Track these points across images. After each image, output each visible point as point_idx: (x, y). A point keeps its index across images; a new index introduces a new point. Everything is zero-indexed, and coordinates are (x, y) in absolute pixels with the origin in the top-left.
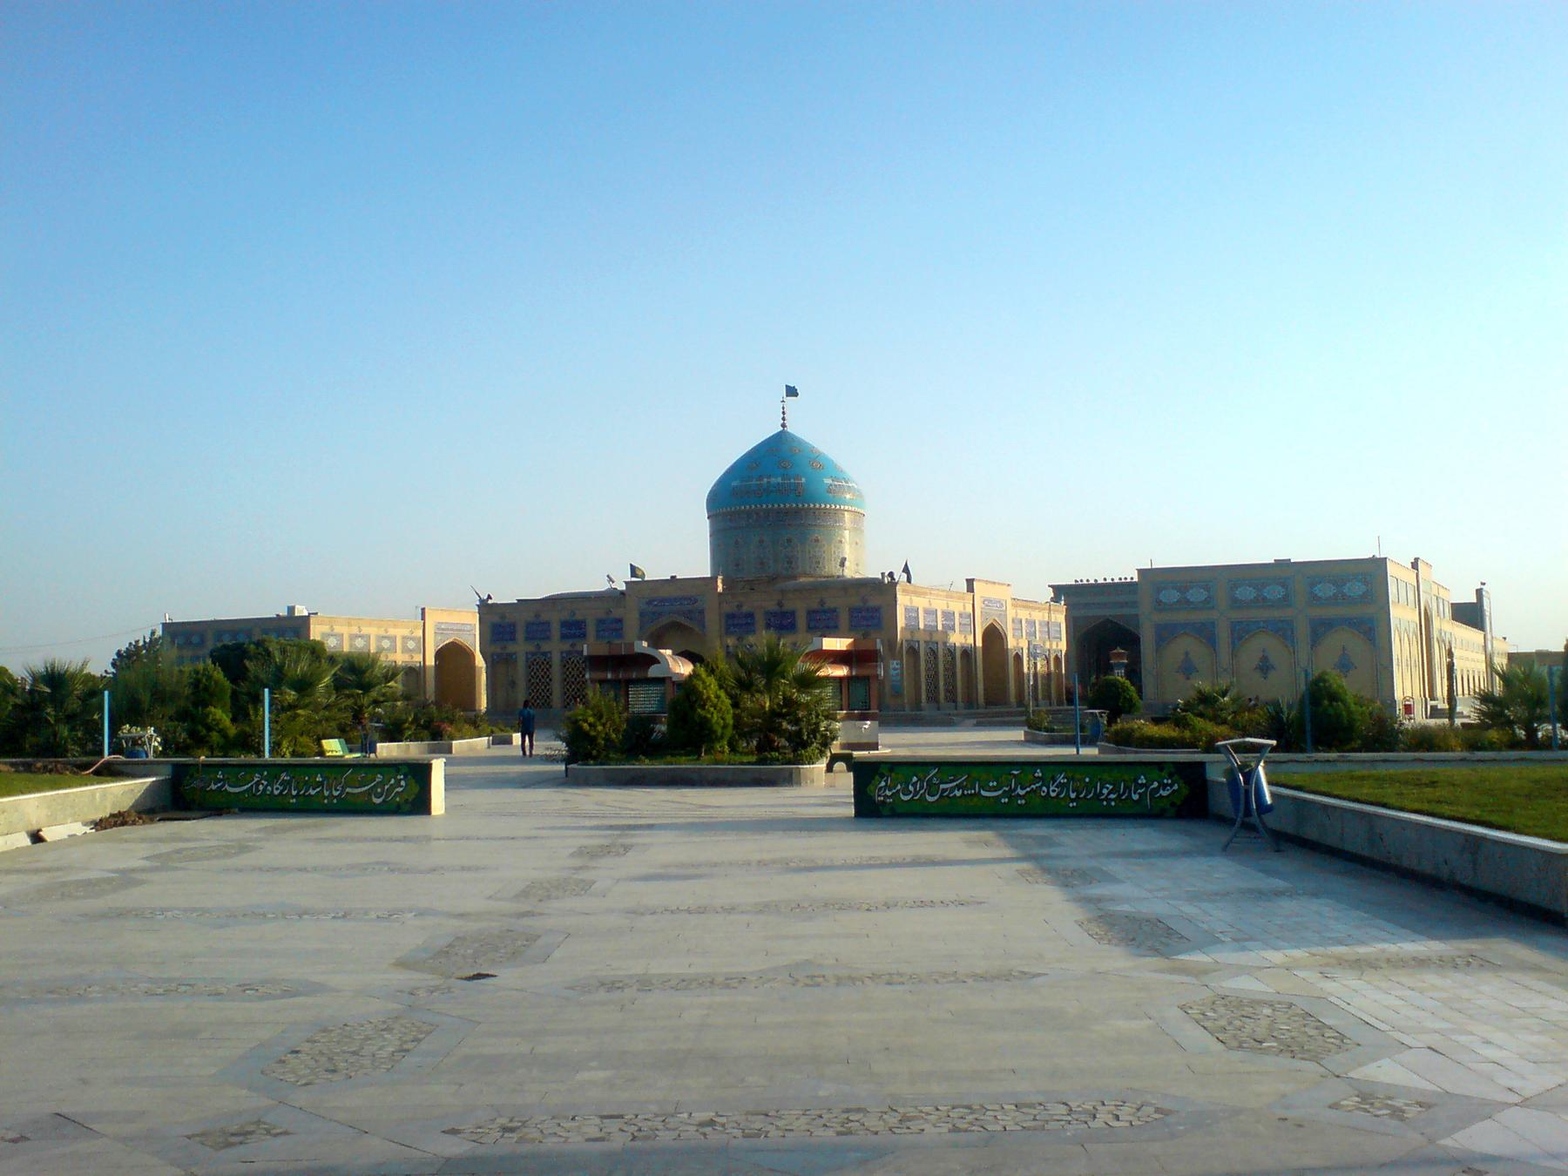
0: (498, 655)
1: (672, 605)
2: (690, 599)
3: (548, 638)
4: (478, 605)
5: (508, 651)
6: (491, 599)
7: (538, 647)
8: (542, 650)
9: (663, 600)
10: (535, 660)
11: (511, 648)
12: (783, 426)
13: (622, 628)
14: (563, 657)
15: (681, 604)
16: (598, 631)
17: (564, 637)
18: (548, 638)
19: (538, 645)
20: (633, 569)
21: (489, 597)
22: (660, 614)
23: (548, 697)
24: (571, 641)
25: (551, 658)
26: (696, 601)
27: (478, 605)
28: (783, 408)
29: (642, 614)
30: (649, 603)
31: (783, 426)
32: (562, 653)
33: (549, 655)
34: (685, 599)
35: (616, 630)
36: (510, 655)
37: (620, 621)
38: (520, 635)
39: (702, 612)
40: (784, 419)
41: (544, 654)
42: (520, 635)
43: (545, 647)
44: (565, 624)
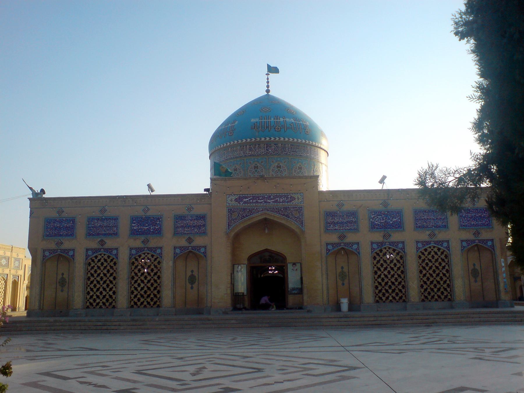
0: (52, 251)
1: (265, 202)
2: (285, 196)
3: (116, 234)
4: (30, 199)
5: (63, 247)
6: (44, 193)
7: (102, 243)
8: (106, 246)
9: (255, 197)
10: (96, 257)
11: (67, 244)
12: (268, 91)
13: (204, 225)
14: (131, 255)
15: (276, 201)
16: (176, 228)
17: (134, 233)
18: (116, 234)
19: (102, 241)
20: (149, 186)
21: (43, 191)
22: (251, 212)
23: (111, 296)
24: (143, 238)
25: (117, 255)
26: (293, 199)
27: (30, 199)
28: (268, 79)
29: (231, 211)
30: (239, 200)
31: (268, 91)
32: (131, 249)
33: (115, 252)
34: (281, 197)
35: (199, 227)
36: (66, 251)
37: (203, 217)
38: (81, 230)
39: (300, 210)
40: (268, 86)
41: (109, 250)
42: (81, 230)
43: (110, 243)
44: (134, 219)
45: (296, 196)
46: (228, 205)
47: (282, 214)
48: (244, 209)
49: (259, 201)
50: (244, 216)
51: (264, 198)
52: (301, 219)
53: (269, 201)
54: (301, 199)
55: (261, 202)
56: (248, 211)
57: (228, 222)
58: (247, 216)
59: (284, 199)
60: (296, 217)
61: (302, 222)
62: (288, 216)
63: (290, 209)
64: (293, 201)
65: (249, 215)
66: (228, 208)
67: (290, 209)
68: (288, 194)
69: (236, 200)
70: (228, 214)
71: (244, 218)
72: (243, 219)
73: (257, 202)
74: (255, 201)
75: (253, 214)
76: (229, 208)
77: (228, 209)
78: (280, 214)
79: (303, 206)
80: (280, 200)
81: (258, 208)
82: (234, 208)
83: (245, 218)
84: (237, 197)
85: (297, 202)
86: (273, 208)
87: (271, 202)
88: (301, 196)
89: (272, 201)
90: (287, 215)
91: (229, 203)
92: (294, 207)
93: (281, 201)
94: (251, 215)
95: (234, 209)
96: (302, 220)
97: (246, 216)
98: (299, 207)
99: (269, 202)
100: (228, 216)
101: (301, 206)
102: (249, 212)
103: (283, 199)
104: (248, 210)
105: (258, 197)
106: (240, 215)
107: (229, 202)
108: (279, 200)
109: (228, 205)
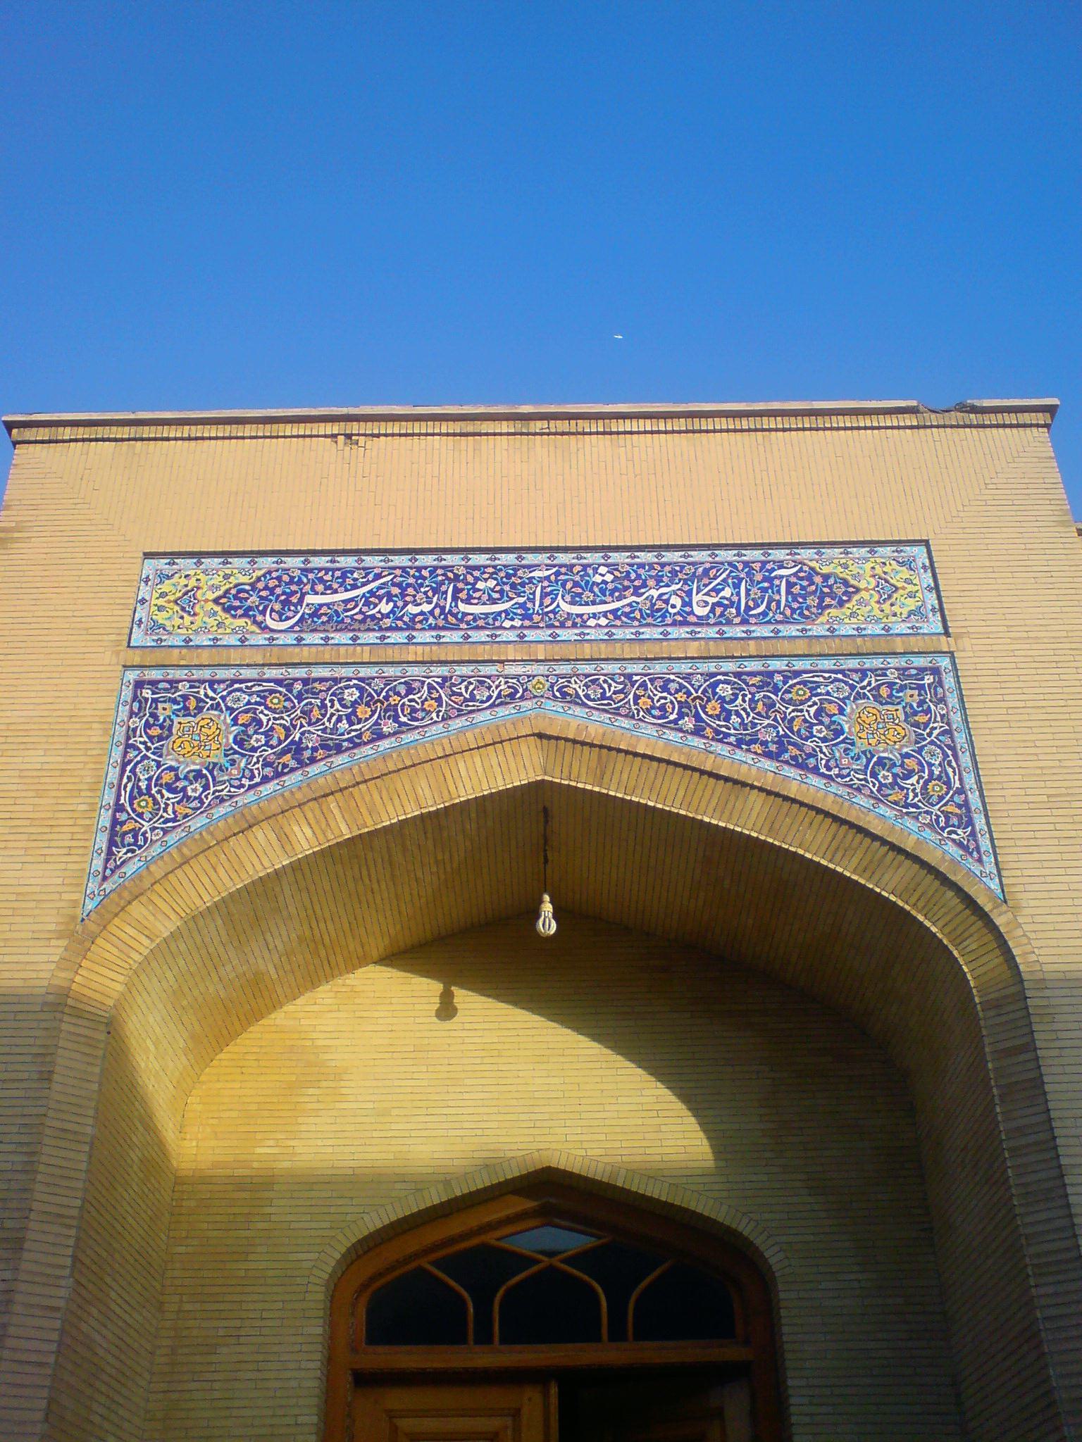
45: (862, 569)
46: (138, 638)
47: (720, 737)
48: (306, 682)
49: (463, 607)
50: (297, 749)
51: (512, 582)
52: (948, 784)
53: (566, 607)
54: (912, 595)
55: (490, 623)
56: (354, 704)
57: (119, 808)
58: (339, 750)
59: (727, 592)
60: (881, 762)
61: (966, 804)
62: (794, 751)
63: (818, 685)
64: (833, 612)
65: (356, 744)
66: (132, 676)
67: (818, 685)
68: (780, 555)
69: (232, 602)
70: (129, 735)
71: (302, 764)
72: (291, 779)
73: (451, 620)
74: (426, 608)
75: (402, 728)
76: (155, 674)
77: (139, 685)
78: (698, 732)
79: (944, 663)
80: (684, 604)
81: (463, 678)
82: (198, 674)
83: (313, 770)
84: (245, 579)
85: (870, 619)
86: (629, 677)
87: (595, 616)
88: (908, 564)
89: (605, 614)
90: (780, 741)
91: (156, 626)
92: (853, 663)
93: (701, 611)
94: (381, 736)
95: (194, 683)
96: (961, 791)
97: (325, 747)
98: (902, 671)
99: (578, 622)
100: (128, 746)
101: (920, 662)
102: (362, 711)
103: (718, 592)
104: (351, 695)
105: (463, 586)
106: (257, 740)
107: (161, 617)
108: (676, 601)
109: (138, 638)
